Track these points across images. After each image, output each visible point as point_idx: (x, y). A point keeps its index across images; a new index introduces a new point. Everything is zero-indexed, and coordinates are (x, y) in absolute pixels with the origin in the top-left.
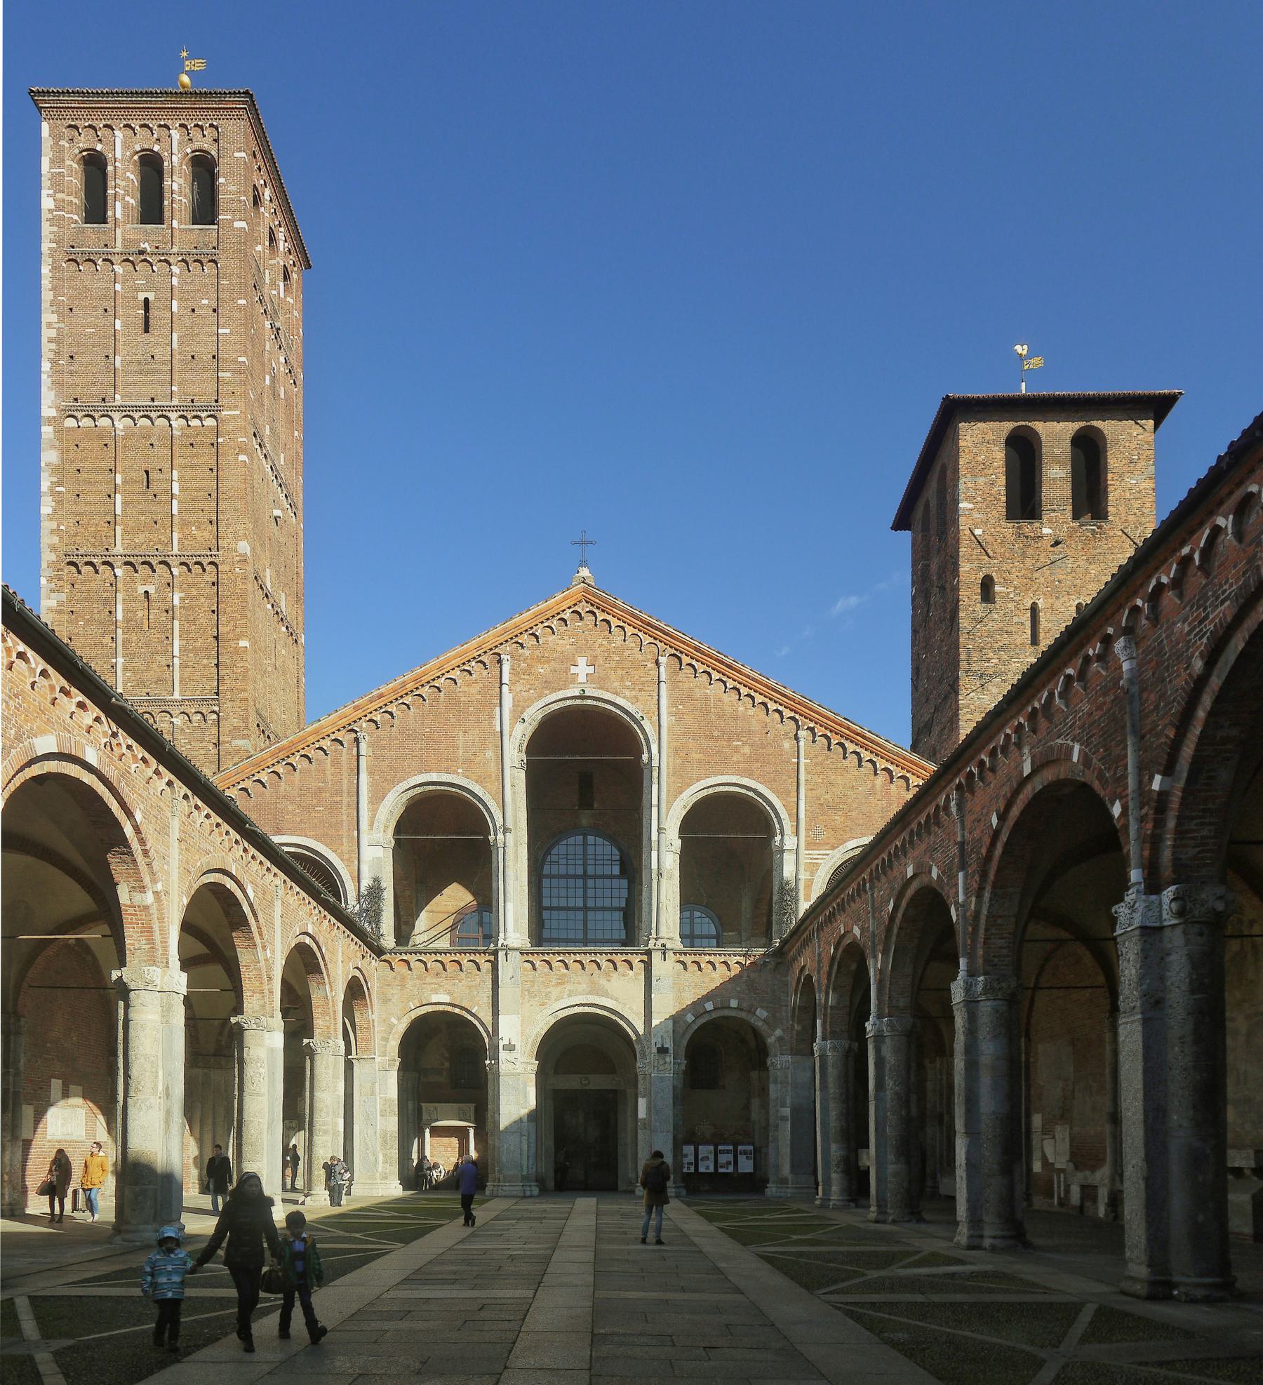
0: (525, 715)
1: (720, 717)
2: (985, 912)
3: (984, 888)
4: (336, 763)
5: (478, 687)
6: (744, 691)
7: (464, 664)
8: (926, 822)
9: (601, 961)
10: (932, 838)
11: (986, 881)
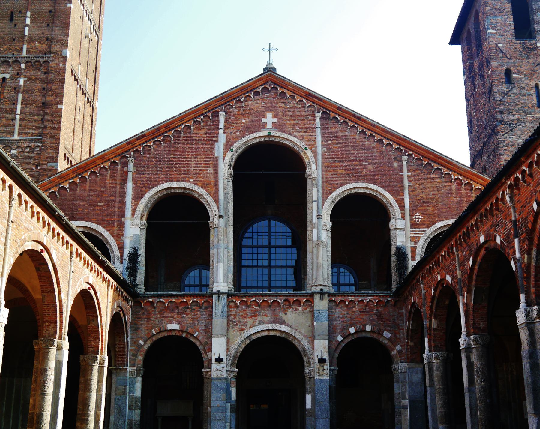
0: (234, 148)
1: (354, 148)
2: (533, 263)
3: (532, 249)
6: (368, 133)
7: (196, 118)
8: (490, 208)
9: (281, 300)
10: (495, 218)
11: (533, 244)
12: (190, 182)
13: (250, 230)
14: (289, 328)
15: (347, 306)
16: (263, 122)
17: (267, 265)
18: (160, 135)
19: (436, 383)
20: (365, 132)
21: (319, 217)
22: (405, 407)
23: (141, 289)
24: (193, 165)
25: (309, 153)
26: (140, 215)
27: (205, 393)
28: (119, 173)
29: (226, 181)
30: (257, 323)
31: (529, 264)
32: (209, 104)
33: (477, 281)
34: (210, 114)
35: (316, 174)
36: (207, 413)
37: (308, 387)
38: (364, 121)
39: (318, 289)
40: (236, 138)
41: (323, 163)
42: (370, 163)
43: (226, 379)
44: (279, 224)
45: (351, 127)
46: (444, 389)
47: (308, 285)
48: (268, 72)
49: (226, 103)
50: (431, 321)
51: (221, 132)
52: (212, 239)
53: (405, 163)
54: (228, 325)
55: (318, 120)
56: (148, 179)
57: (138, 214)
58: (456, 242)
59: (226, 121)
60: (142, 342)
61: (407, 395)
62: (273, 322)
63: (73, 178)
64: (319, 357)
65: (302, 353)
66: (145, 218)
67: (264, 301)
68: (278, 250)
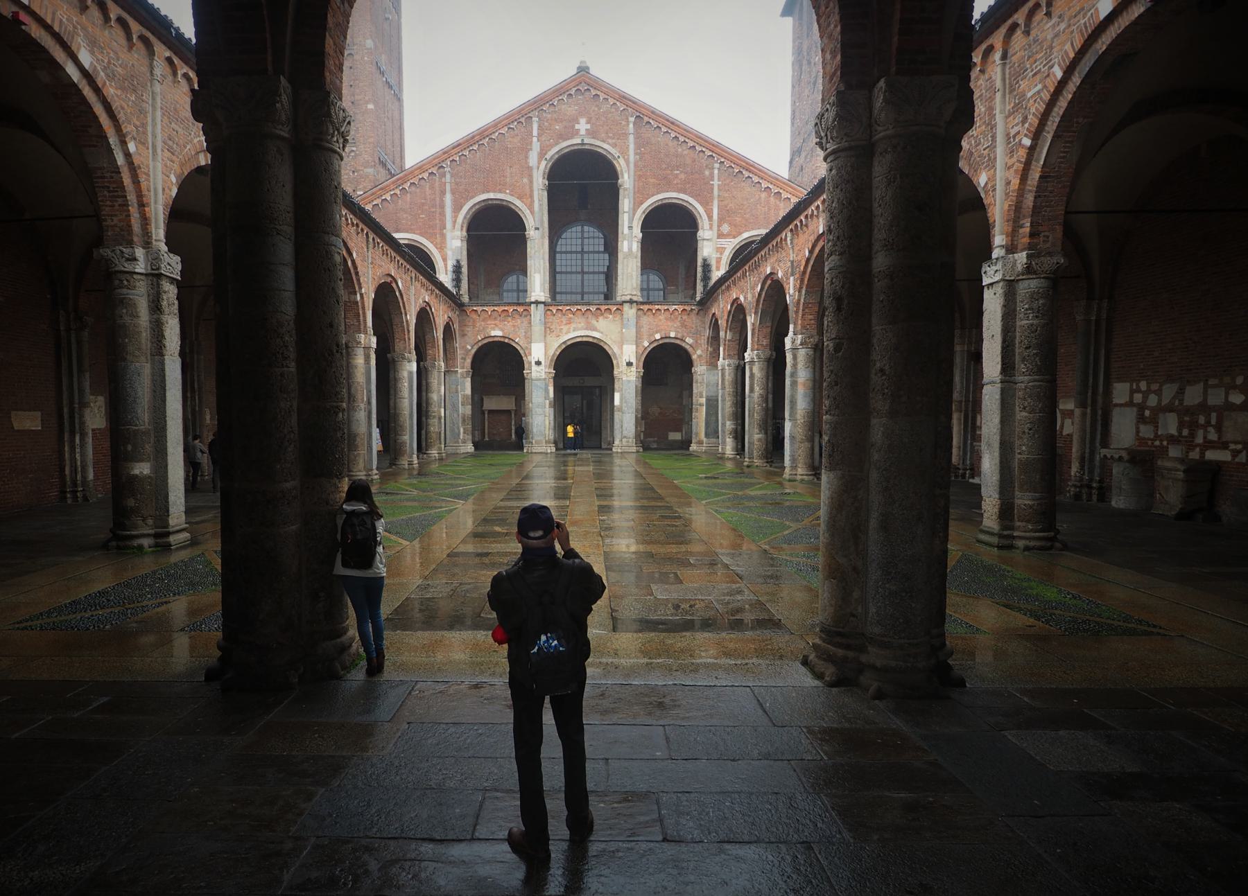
2: (802, 300)
4: (432, 187)
5: (519, 138)
7: (509, 124)
8: (776, 245)
12: (506, 193)
13: (564, 236)
14: (601, 334)
15: (654, 314)
16: (576, 128)
17: (580, 270)
18: (474, 143)
19: (727, 387)
20: (678, 138)
21: (630, 228)
22: (701, 405)
23: (466, 299)
24: (508, 176)
25: (622, 161)
26: (460, 228)
27: (527, 391)
28: (437, 184)
29: (540, 192)
30: (572, 329)
31: (799, 300)
32: (523, 109)
33: (763, 305)
34: (523, 120)
35: (628, 184)
36: (529, 408)
37: (616, 386)
38: (678, 126)
39: (628, 298)
40: (550, 145)
41: (635, 172)
42: (681, 172)
43: (545, 379)
44: (591, 229)
45: (665, 132)
46: (733, 392)
47: (618, 294)
48: (581, 71)
49: (538, 107)
50: (726, 332)
51: (535, 139)
52: (528, 250)
53: (716, 172)
54: (545, 332)
55: (631, 126)
56: (466, 190)
57: (458, 226)
58: (749, 267)
59: (540, 127)
60: (469, 347)
61: (704, 394)
62: (586, 329)
63: (393, 189)
64: (628, 361)
65: (612, 357)
66: (465, 229)
67: (578, 310)
68: (591, 255)
